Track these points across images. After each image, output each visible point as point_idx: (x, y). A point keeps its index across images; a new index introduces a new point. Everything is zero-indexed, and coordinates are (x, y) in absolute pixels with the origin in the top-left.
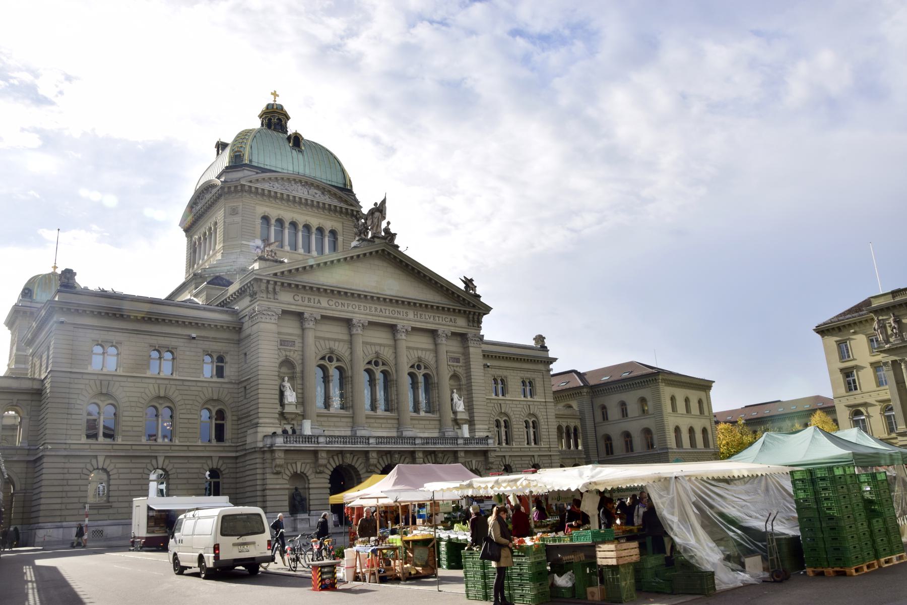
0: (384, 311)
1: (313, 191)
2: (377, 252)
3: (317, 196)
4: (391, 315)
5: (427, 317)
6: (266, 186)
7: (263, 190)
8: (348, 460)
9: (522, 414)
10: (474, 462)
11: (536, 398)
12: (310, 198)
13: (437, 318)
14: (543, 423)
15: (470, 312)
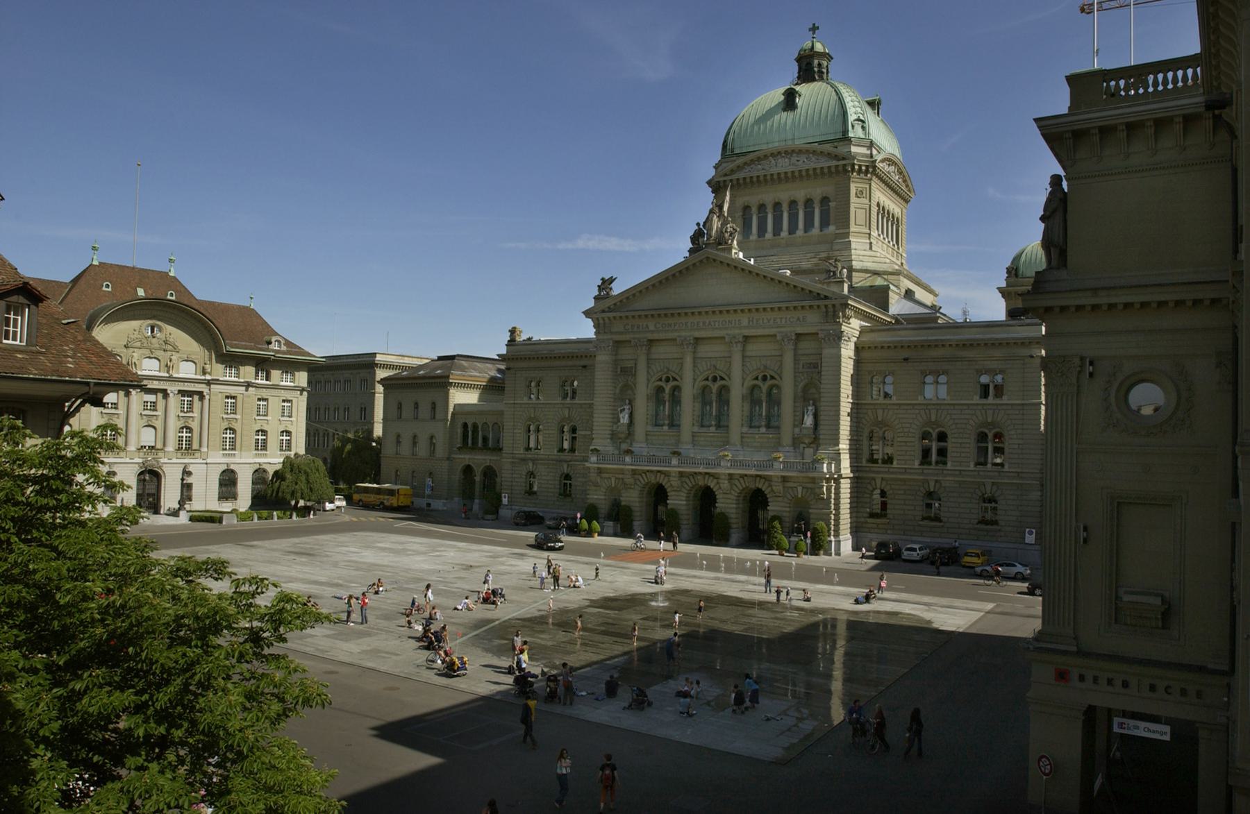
0: (713, 324)
1: (794, 159)
2: (701, 261)
3: (800, 163)
4: (721, 326)
5: (765, 321)
6: (741, 175)
7: (738, 179)
8: (653, 479)
9: (971, 422)
10: (800, 489)
11: (1005, 399)
12: (789, 169)
13: (778, 320)
14: (1015, 436)
15: (818, 306)
